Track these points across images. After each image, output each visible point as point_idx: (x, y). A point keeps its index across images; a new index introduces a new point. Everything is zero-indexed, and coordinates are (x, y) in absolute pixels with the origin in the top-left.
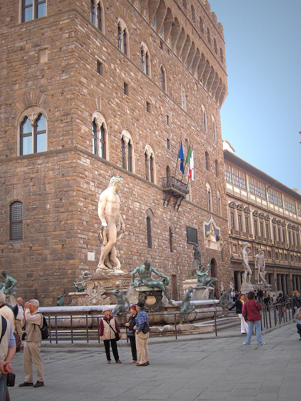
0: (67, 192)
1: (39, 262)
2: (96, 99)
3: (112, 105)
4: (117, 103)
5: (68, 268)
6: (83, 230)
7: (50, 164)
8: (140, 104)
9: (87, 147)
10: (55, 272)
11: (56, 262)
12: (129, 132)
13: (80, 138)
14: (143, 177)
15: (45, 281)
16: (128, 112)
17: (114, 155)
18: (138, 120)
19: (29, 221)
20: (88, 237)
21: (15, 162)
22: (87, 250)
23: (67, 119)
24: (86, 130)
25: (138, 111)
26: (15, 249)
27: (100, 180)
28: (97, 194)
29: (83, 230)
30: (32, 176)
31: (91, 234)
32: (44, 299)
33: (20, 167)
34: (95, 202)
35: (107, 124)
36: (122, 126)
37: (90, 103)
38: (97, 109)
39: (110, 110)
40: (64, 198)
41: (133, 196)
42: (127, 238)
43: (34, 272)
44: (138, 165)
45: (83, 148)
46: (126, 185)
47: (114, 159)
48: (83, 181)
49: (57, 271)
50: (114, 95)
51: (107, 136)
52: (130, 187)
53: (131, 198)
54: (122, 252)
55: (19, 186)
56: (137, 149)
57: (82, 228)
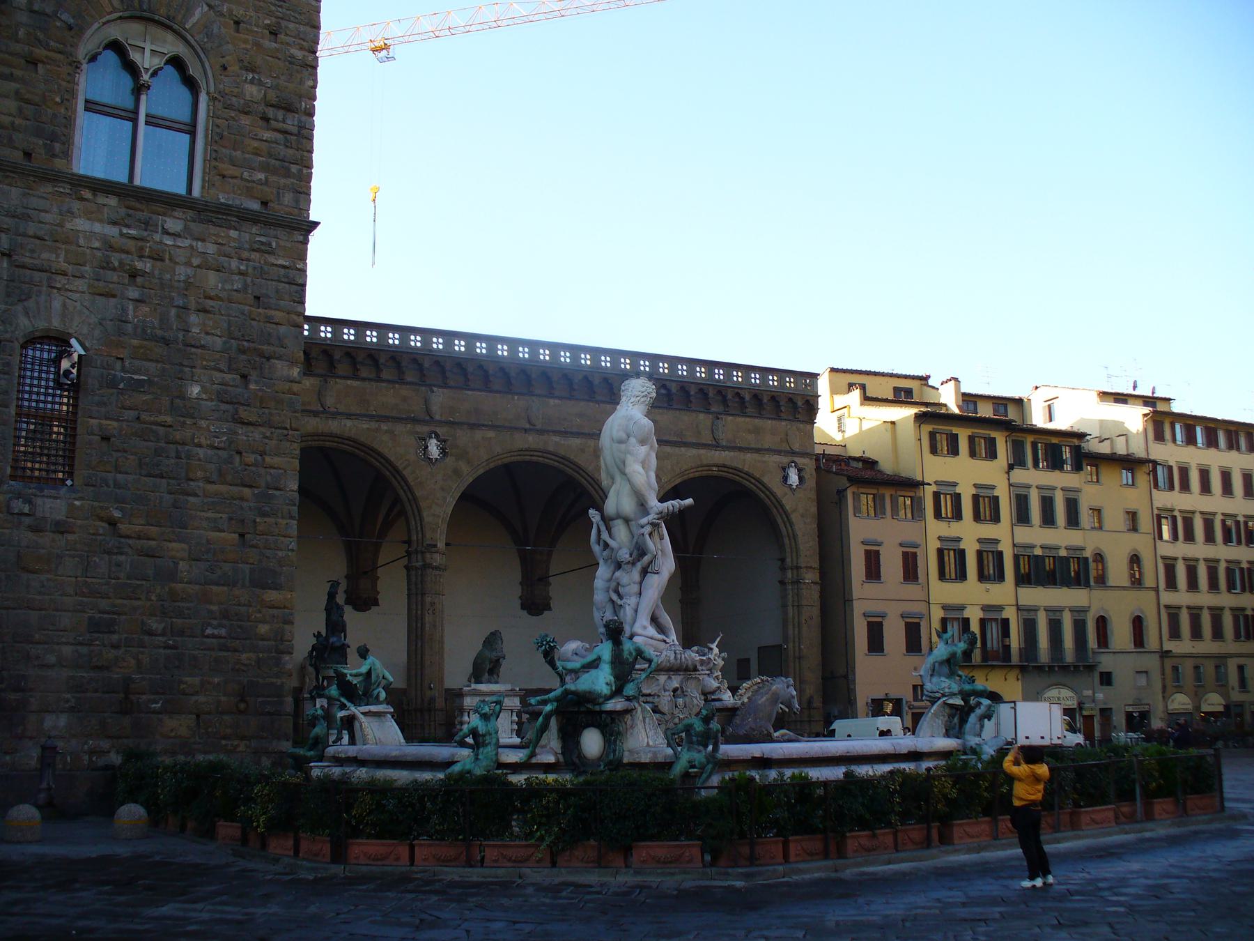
0: (268, 359)
1: (144, 582)
5: (258, 615)
10: (209, 625)
11: (215, 588)
15: (168, 651)
19: (115, 424)
21: (68, 191)
23: (284, 121)
26: (44, 518)
30: (139, 265)
32: (160, 716)
33: (89, 215)
40: (254, 376)
43: (119, 614)
49: (215, 622)
55: (80, 284)
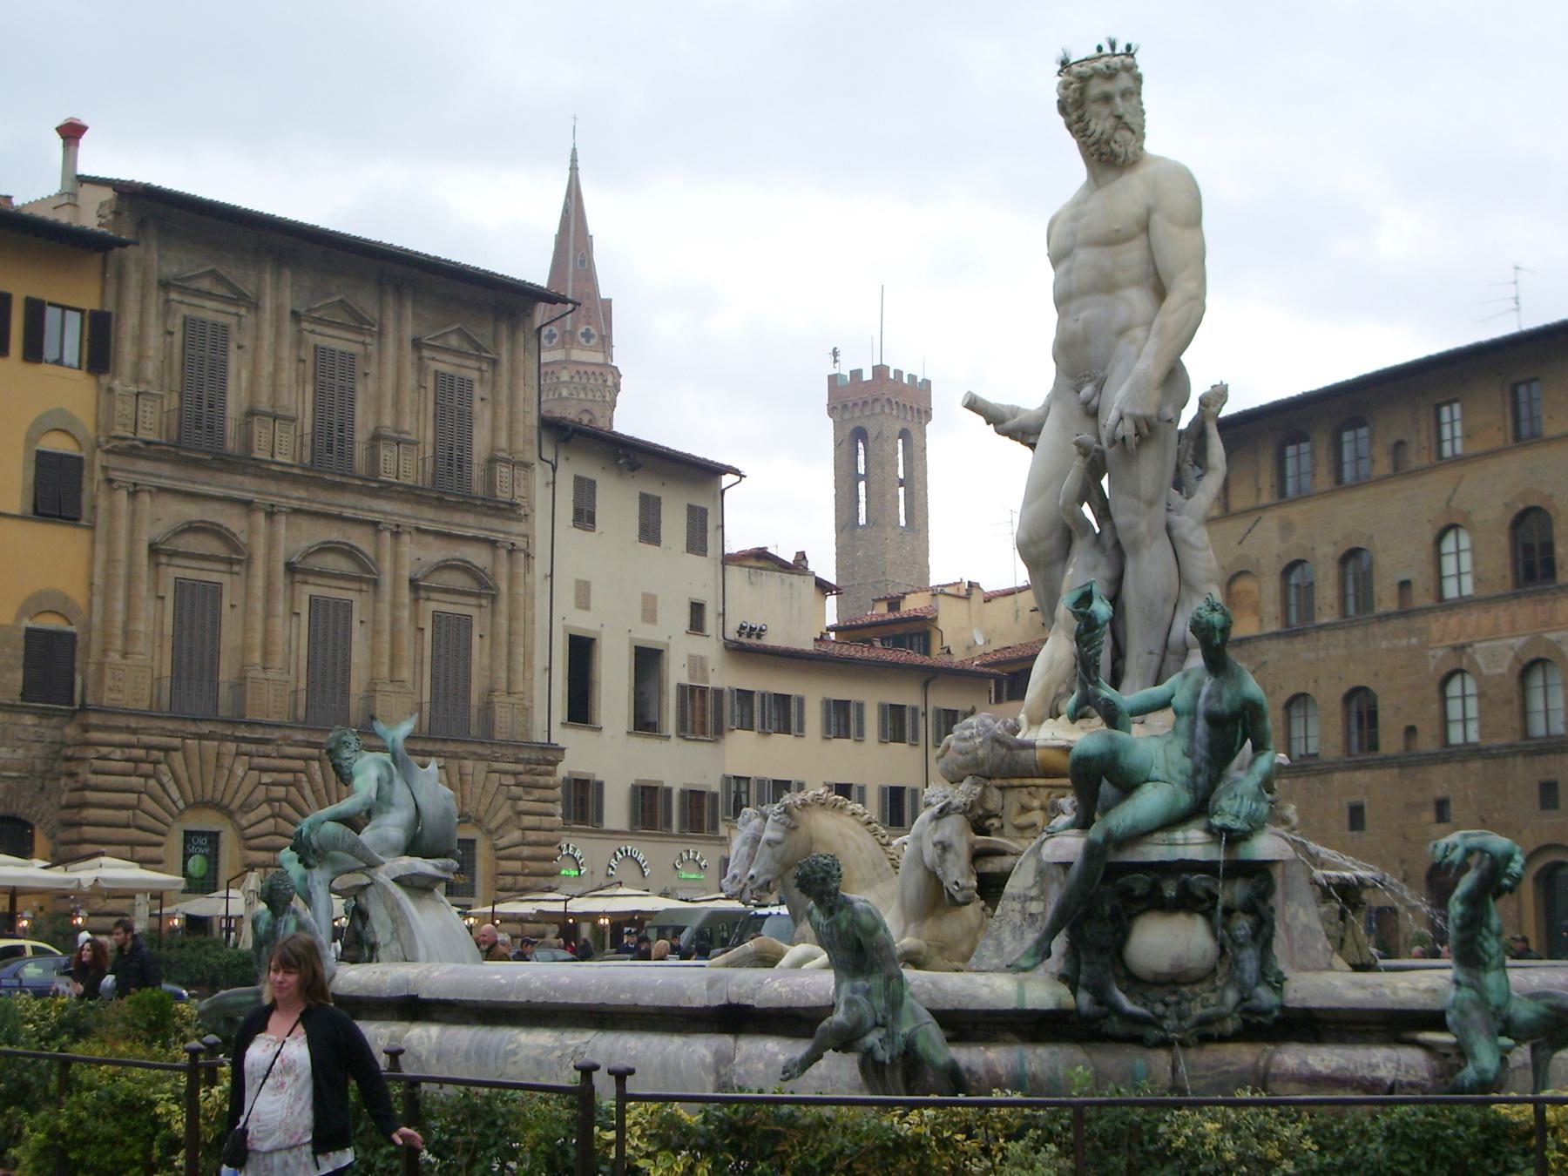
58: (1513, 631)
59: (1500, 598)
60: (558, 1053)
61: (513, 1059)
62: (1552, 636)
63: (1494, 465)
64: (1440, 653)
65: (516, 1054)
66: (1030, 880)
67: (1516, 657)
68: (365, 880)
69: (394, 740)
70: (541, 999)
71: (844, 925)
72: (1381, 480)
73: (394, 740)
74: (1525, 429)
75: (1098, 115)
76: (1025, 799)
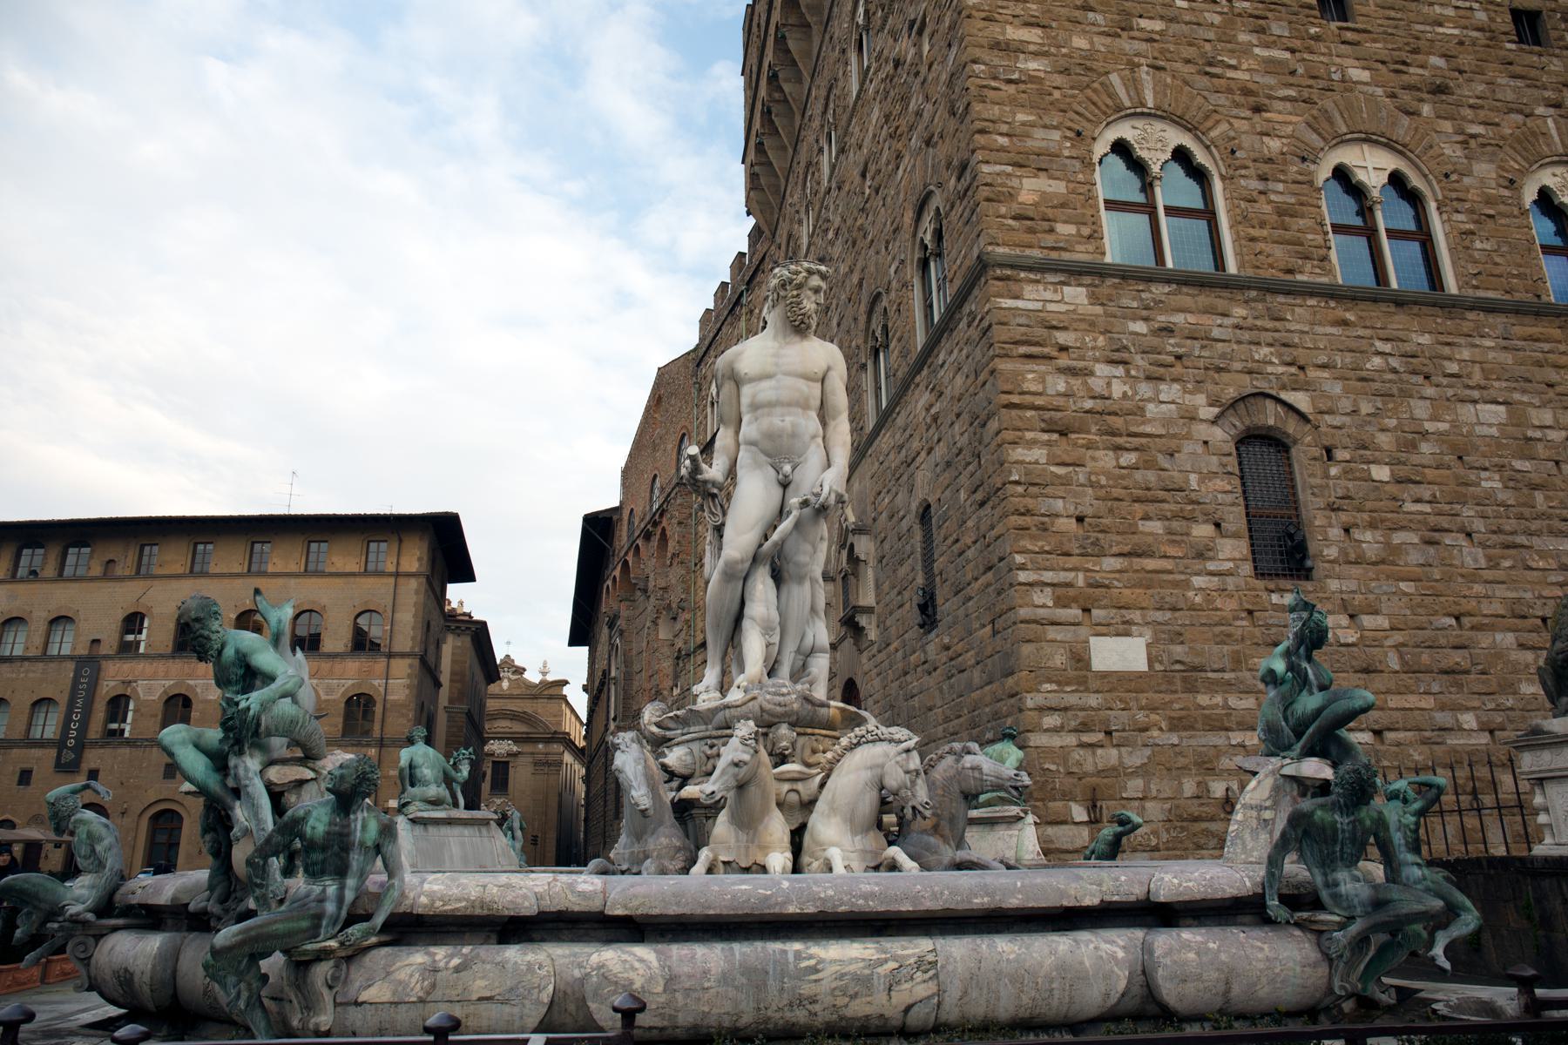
2: (1115, 78)
3: (1230, 74)
4: (1269, 61)
6: (1048, 553)
7: (956, 351)
8: (1456, 32)
9: (1061, 245)
12: (1386, 145)
13: (1010, 222)
14: (1529, 297)
16: (1358, 74)
17: (1260, 246)
18: (1440, 90)
20: (1086, 578)
22: (1083, 631)
24: (1051, 190)
25: (1444, 56)
27: (1171, 349)
28: (1151, 407)
29: (1048, 553)
31: (1111, 563)
34: (1129, 435)
35: (1207, 147)
36: (1319, 134)
37: (1073, 96)
38: (1119, 108)
39: (1213, 98)
41: (1445, 381)
42: (1414, 557)
44: (1471, 256)
45: (1036, 253)
46: (1380, 345)
47: (1270, 260)
48: (1043, 368)
50: (1243, 37)
51: (1218, 186)
52: (1408, 347)
53: (1430, 391)
54: (1367, 621)
55: (923, 454)
56: (1454, 195)
57: (1040, 544)
58: (166, 677)
59: (162, 656)
60: (892, 965)
61: (814, 977)
62: (191, 682)
63: (175, 584)
64: (112, 684)
65: (817, 971)
66: (1266, 794)
67: (165, 692)
68: (310, 775)
69: (280, 621)
70: (842, 909)
71: (1368, 823)
72: (93, 579)
73: (280, 621)
74: (197, 568)
75: (809, 298)
76: (815, 744)
